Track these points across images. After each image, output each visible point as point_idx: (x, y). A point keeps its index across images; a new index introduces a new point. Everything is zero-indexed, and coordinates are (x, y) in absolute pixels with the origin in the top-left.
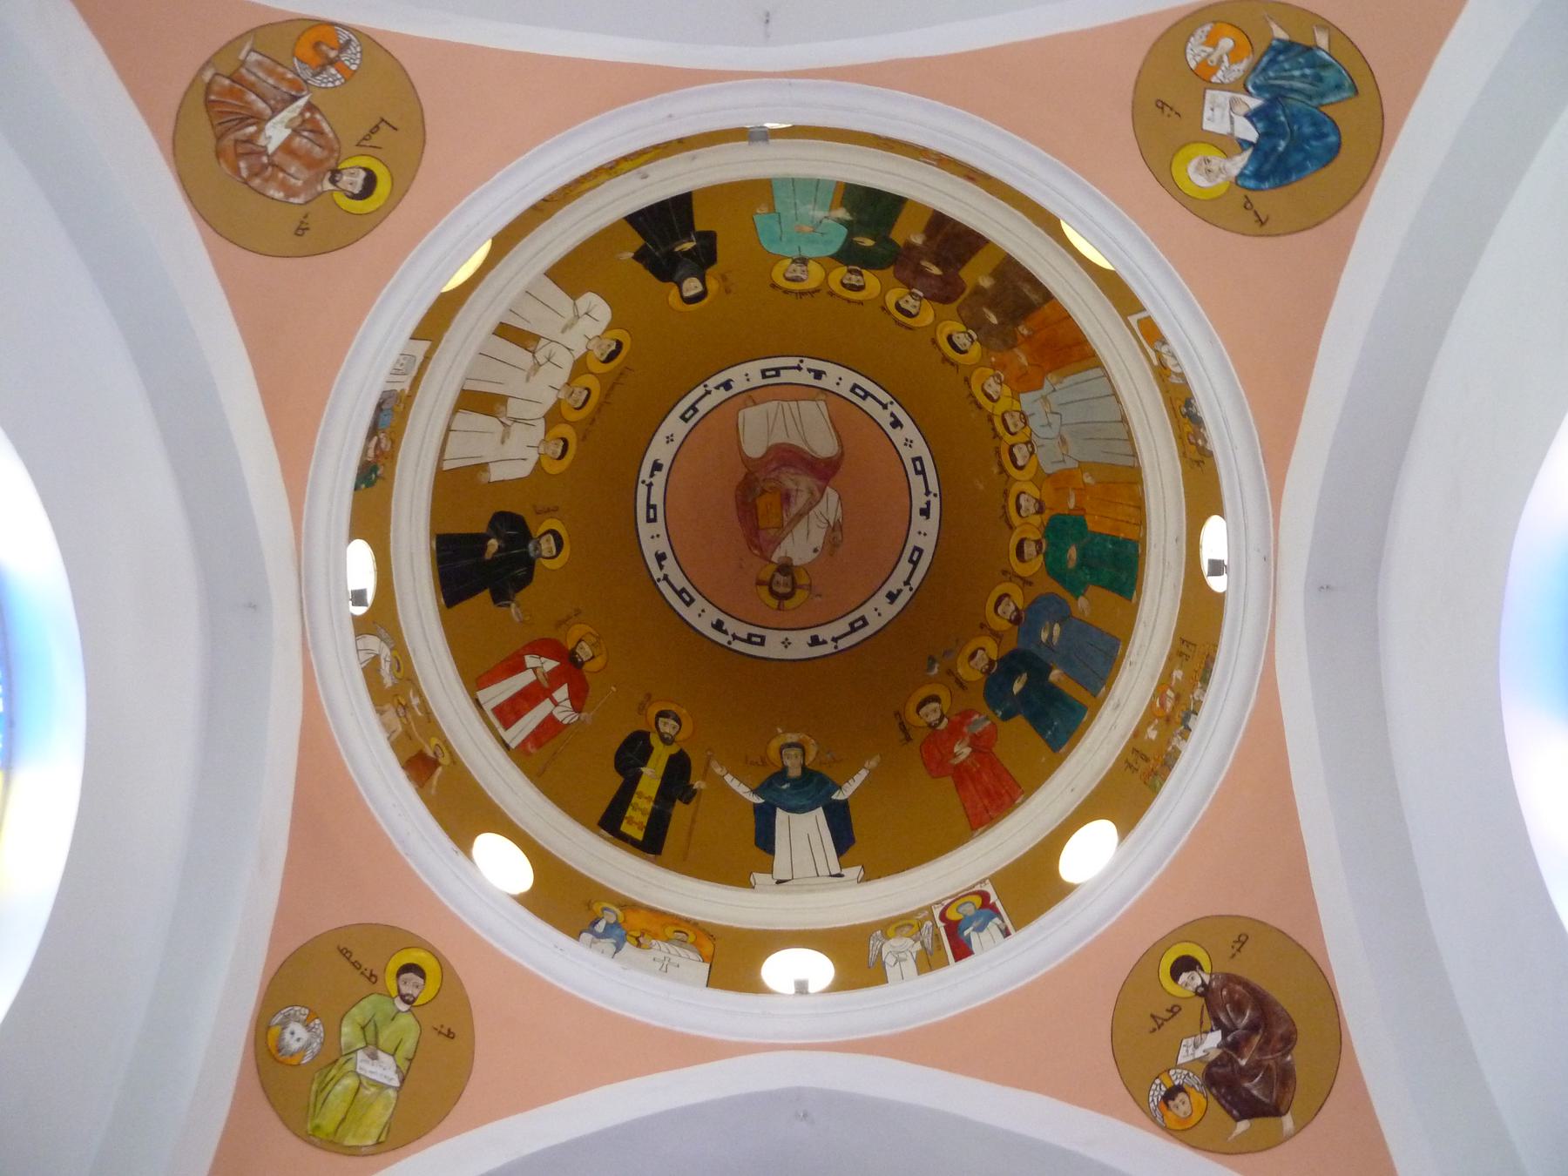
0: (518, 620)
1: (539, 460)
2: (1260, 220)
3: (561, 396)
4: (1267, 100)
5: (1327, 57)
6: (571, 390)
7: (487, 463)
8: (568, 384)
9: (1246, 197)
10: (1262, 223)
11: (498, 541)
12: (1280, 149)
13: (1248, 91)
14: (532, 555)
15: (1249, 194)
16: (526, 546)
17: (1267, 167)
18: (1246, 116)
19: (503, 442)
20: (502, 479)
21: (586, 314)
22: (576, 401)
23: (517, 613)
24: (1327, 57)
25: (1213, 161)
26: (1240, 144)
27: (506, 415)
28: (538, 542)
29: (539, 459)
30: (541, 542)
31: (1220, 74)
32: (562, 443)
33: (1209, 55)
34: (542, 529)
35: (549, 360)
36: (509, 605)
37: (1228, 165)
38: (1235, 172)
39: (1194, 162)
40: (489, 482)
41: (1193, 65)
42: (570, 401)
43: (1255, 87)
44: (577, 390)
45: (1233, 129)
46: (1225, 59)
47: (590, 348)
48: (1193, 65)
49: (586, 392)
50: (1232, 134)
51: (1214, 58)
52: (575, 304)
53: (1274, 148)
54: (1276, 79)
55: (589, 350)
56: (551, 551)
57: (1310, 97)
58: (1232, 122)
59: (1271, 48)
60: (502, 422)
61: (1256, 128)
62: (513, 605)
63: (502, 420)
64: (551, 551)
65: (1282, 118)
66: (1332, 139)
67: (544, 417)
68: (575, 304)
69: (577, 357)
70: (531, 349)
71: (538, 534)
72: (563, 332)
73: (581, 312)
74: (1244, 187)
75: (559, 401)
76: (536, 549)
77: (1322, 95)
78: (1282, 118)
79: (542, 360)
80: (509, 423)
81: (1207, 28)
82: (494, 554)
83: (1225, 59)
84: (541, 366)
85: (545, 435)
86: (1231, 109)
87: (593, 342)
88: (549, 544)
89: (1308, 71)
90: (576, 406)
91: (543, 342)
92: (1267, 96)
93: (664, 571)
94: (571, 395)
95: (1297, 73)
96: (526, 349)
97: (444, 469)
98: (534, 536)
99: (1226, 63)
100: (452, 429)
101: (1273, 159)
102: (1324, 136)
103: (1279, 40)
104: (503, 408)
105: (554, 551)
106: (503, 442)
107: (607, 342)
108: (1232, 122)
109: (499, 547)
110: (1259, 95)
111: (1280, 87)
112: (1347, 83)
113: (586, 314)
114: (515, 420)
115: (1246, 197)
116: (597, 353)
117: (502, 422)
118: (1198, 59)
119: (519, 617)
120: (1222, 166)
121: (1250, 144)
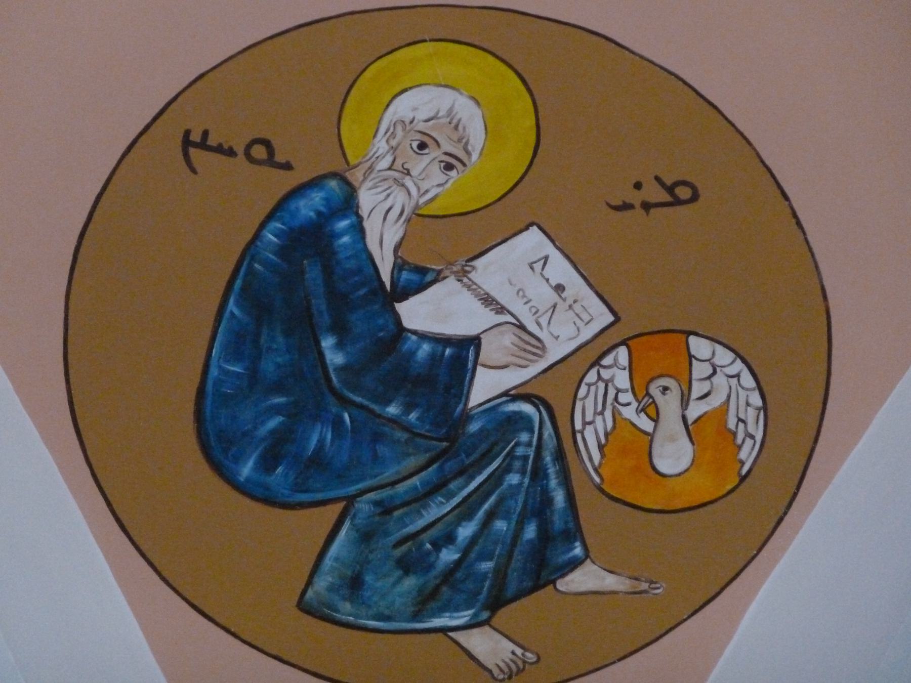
2: (203, 145)
4: (467, 417)
5: (437, 622)
9: (287, 166)
10: (187, 142)
12: (327, 343)
13: (527, 398)
15: (290, 181)
17: (313, 274)
18: (475, 341)
24: (437, 622)
25: (438, 176)
26: (422, 271)
31: (622, 380)
33: (685, 401)
37: (399, 199)
38: (367, 199)
39: (476, 135)
41: (699, 347)
43: (518, 422)
45: (472, 287)
46: (646, 424)
48: (699, 347)
50: (462, 275)
51: (669, 405)
53: (341, 330)
54: (496, 479)
57: (386, 509)
58: (488, 300)
59: (574, 533)
61: (423, 336)
65: (393, 410)
66: (246, 470)
74: (315, 183)
77: (366, 537)
78: (393, 410)
81: (747, 454)
83: (646, 424)
86: (522, 327)
89: (448, 556)
92: (474, 427)
95: (465, 532)
99: (629, 413)
101: (320, 304)
102: (268, 462)
103: (574, 564)
108: (488, 300)
110: (491, 408)
111: (468, 472)
112: (346, 610)
115: (287, 166)
118: (700, 370)
120: (408, 182)
121: (404, 293)
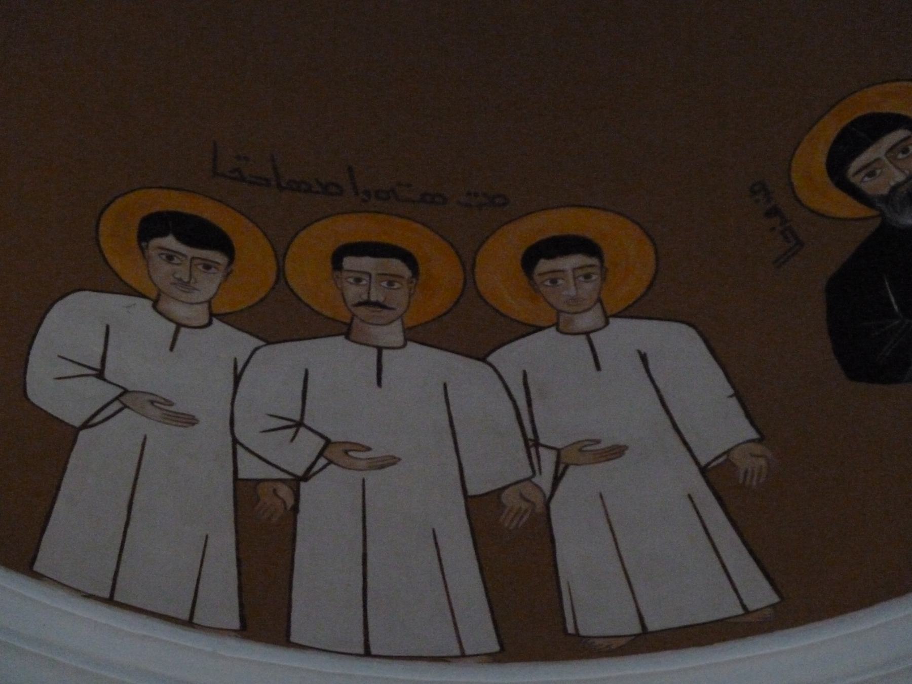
1: (629, 312)
3: (393, 334)
6: (362, 312)
7: (704, 470)
8: (347, 331)
19: (617, 451)
20: (734, 402)
21: (100, 374)
22: (391, 280)
27: (529, 479)
28: (886, 199)
29: (615, 316)
30: (885, 191)
32: (544, 265)
34: (846, 206)
35: (299, 424)
40: (761, 440)
42: (399, 297)
44: (354, 293)
47: (199, 314)
49: (349, 262)
52: (86, 425)
55: (212, 315)
60: (557, 479)
63: (546, 486)
67: (483, 359)
68: (86, 425)
69: (255, 342)
70: (284, 492)
72: (190, 421)
73: (100, 393)
75: (412, 335)
79: (309, 445)
80: (548, 459)
84: (328, 442)
85: (540, 329)
87: (181, 311)
88: (877, 160)
90: (407, 272)
91: (250, 469)
94: (382, 306)
96: (295, 509)
97: (774, 599)
98: (877, 223)
100: (637, 629)
104: (510, 499)
106: (617, 451)
107: (163, 270)
113: (100, 374)
114: (532, 444)
116: (208, 285)
117: (557, 479)
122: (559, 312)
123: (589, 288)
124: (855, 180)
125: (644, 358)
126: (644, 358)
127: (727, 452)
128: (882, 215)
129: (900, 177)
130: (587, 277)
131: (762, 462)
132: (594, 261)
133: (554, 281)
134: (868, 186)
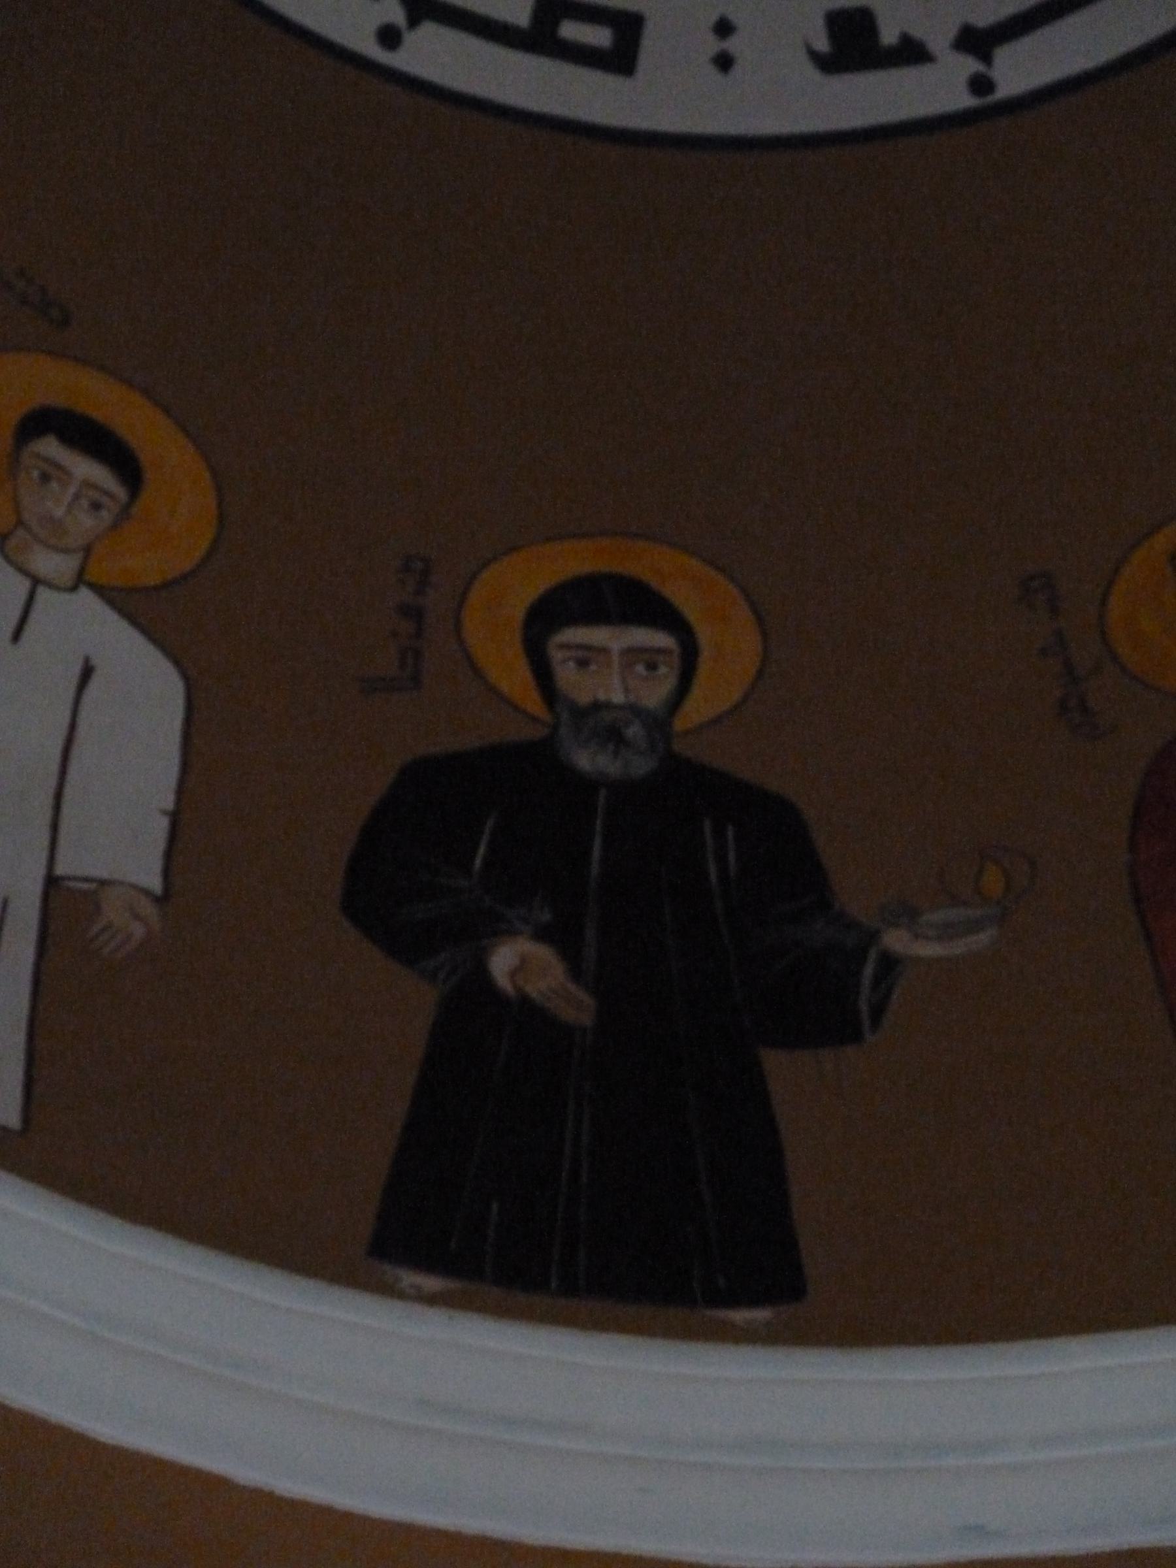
0: (982, 939)
7: (52, 882)
11: (512, 933)
14: (641, 766)
16: (588, 785)
20: (162, 824)
23: (948, 932)
29: (92, 586)
30: (584, 698)
32: (50, 447)
36: (890, 964)
40: (162, 900)
56: (651, 659)
62: (896, 940)
64: (651, 659)
71: (534, 703)
76: (614, 737)
82: (576, 972)
88: (604, 651)
93: (939, 39)
98: (537, 733)
105: (662, 639)
109: (542, 935)
119: (974, 926)
122: (20, 523)
123: (86, 523)
124: (556, 655)
125: (87, 673)
126: (87, 673)
127: (103, 883)
128: (555, 728)
129: (618, 698)
130: (96, 506)
131: (138, 930)
132: (121, 492)
133: (45, 478)
134: (566, 674)
